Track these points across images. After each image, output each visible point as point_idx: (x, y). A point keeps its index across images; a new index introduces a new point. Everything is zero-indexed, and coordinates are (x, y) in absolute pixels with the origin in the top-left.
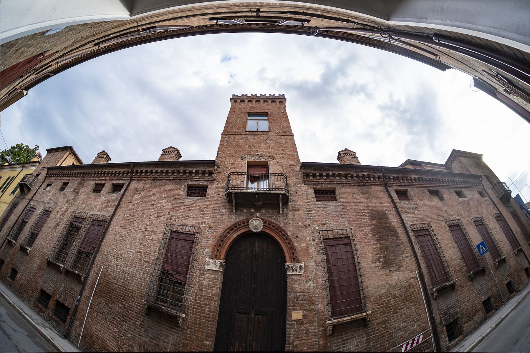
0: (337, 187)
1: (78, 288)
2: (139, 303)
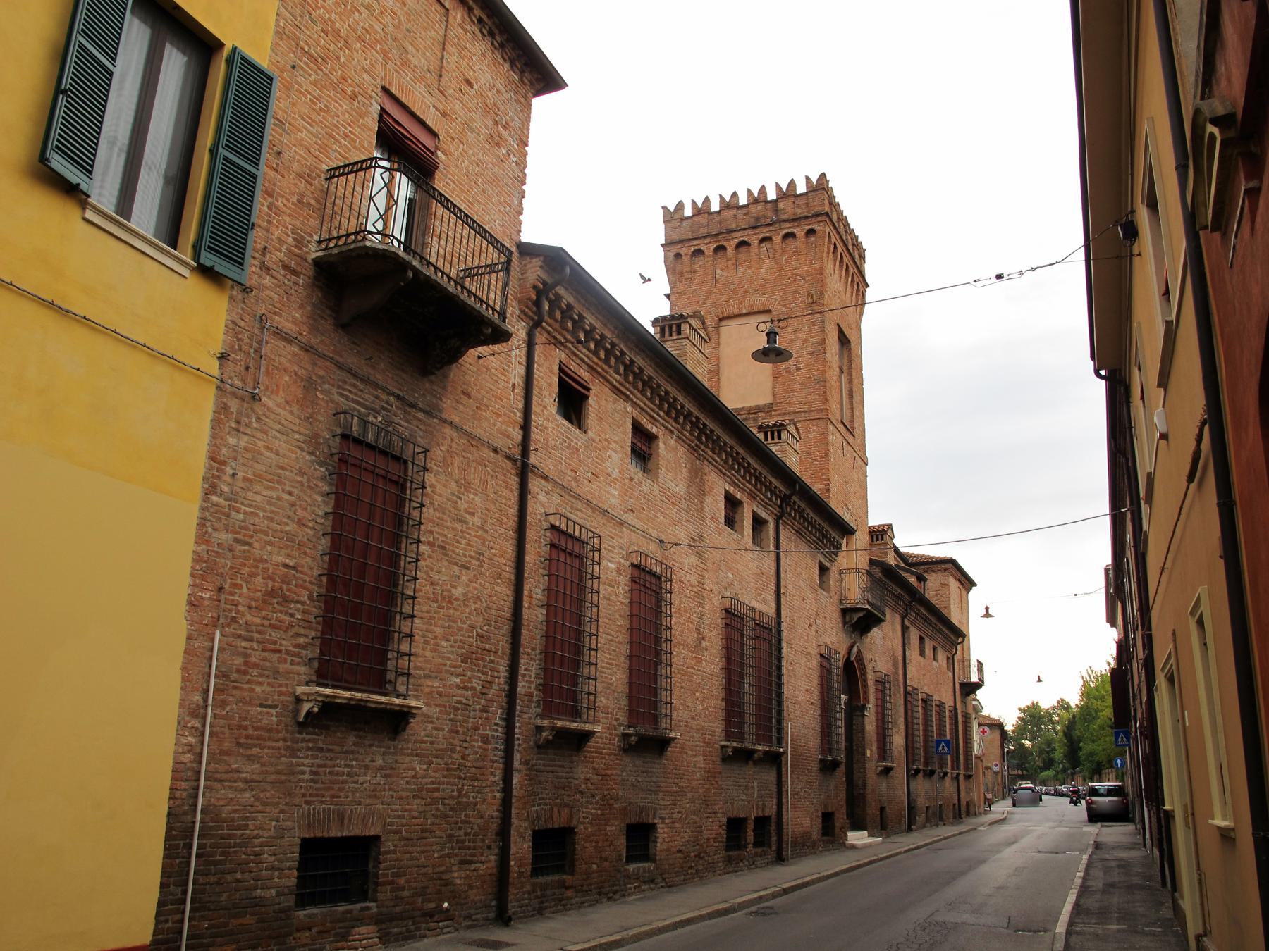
1: (771, 776)
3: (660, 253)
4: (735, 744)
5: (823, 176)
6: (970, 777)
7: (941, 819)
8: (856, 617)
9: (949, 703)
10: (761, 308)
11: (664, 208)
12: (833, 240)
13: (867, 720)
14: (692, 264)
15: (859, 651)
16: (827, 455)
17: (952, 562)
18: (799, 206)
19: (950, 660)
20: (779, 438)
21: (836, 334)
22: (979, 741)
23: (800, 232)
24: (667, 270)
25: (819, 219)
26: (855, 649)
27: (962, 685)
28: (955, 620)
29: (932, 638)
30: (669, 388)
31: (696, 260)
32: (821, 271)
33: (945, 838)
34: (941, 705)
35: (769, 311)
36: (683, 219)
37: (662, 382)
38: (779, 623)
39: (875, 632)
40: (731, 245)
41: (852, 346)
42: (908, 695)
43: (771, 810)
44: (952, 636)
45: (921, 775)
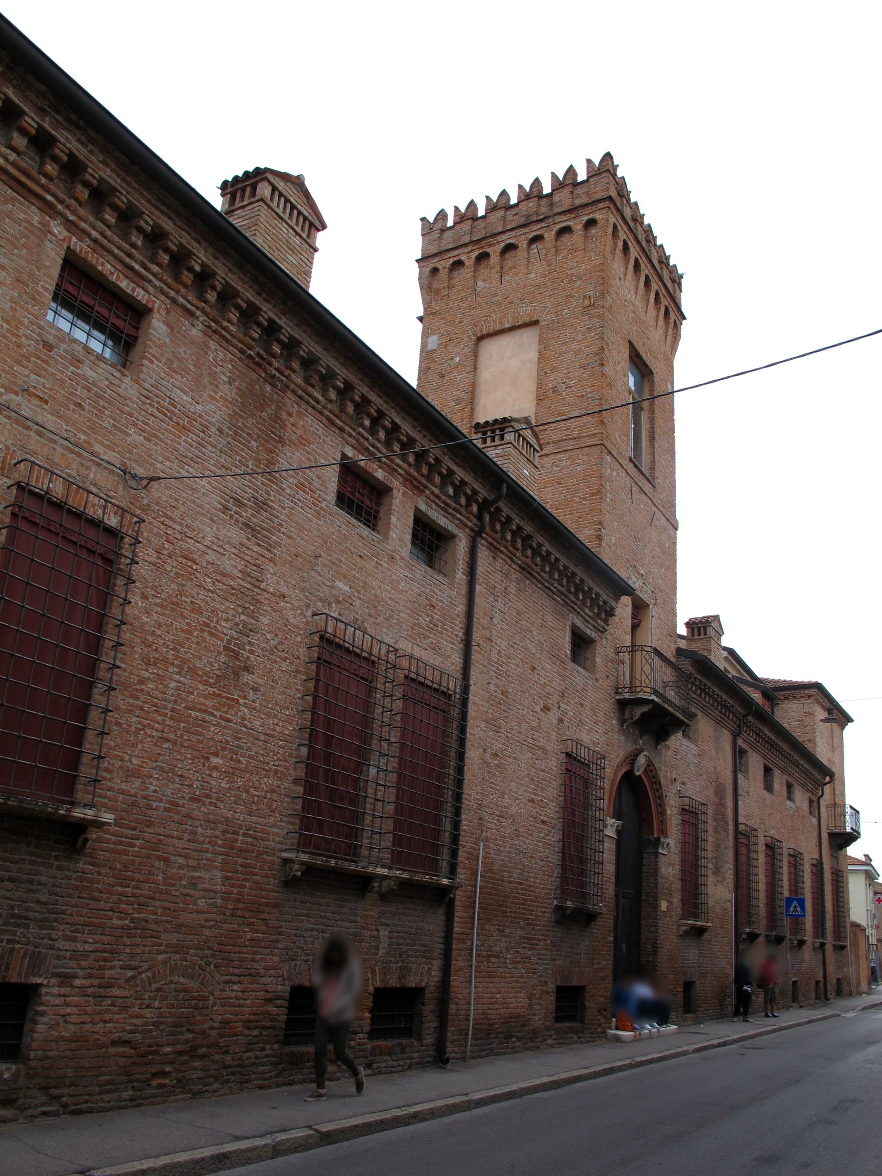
0: (700, 715)
1: (434, 922)
2: (545, 908)
3: (415, 269)
4: (304, 857)
5: (608, 156)
6: (843, 948)
7: (795, 999)
8: (639, 712)
9: (809, 854)
10: (528, 320)
11: (423, 219)
12: (622, 236)
13: (662, 861)
14: (450, 278)
15: (650, 764)
16: (599, 492)
17: (818, 687)
18: (578, 196)
19: (814, 804)
20: (502, 437)
21: (625, 353)
22: (859, 906)
23: (577, 225)
24: (422, 288)
25: (601, 205)
26: (642, 760)
27: (831, 835)
28: (822, 753)
29: (783, 771)
30: (168, 225)
31: (455, 274)
32: (603, 267)
33: (782, 1029)
34: (796, 857)
35: (535, 323)
36: (444, 230)
37: (144, 206)
38: (466, 689)
39: (676, 740)
40: (494, 251)
41: (656, 379)
42: (743, 838)
43: (424, 974)
44: (817, 776)
45: (761, 939)
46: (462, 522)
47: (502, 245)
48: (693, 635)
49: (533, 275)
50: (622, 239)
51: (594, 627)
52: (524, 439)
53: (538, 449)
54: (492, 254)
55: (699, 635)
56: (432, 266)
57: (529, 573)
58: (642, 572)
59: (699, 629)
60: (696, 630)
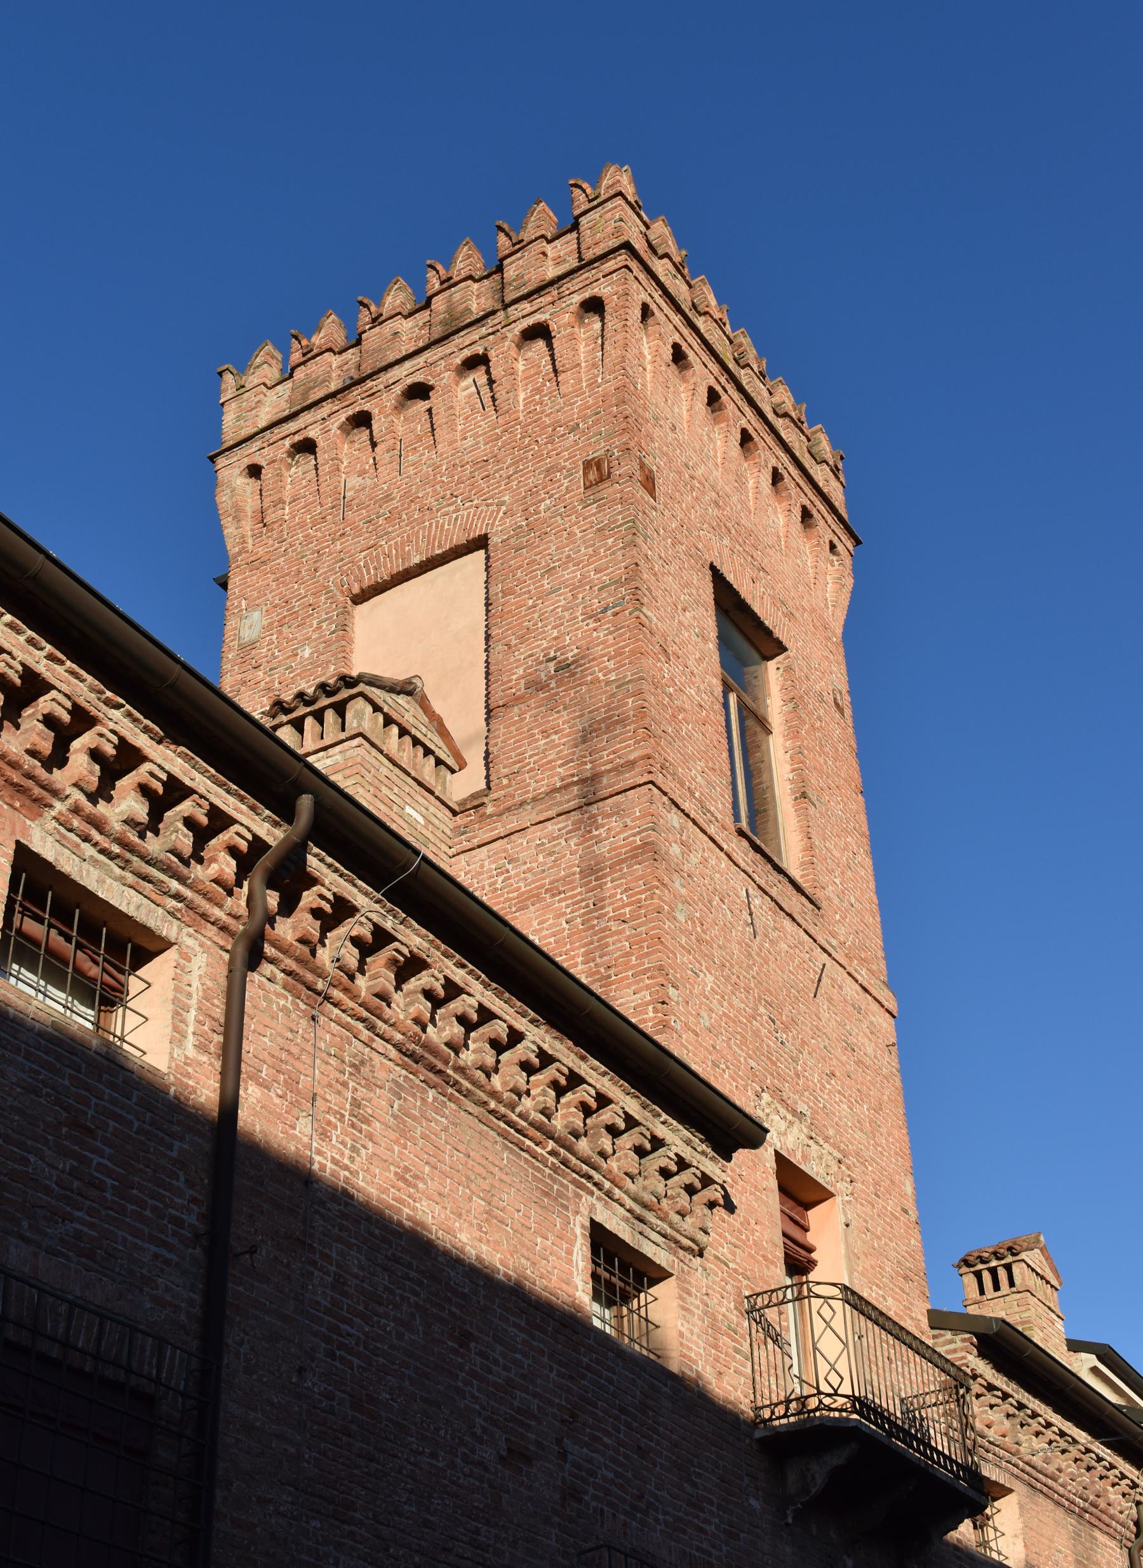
8: (819, 1472)
25: (610, 265)
35: (481, 543)
40: (381, 404)
46: (190, 906)
47: (398, 389)
48: (982, 1292)
49: (470, 442)
50: (671, 341)
51: (664, 1236)
52: (403, 732)
53: (450, 761)
54: (375, 412)
55: (997, 1287)
56: (247, 461)
57: (431, 1068)
58: (802, 1107)
59: (993, 1271)
60: (986, 1276)
